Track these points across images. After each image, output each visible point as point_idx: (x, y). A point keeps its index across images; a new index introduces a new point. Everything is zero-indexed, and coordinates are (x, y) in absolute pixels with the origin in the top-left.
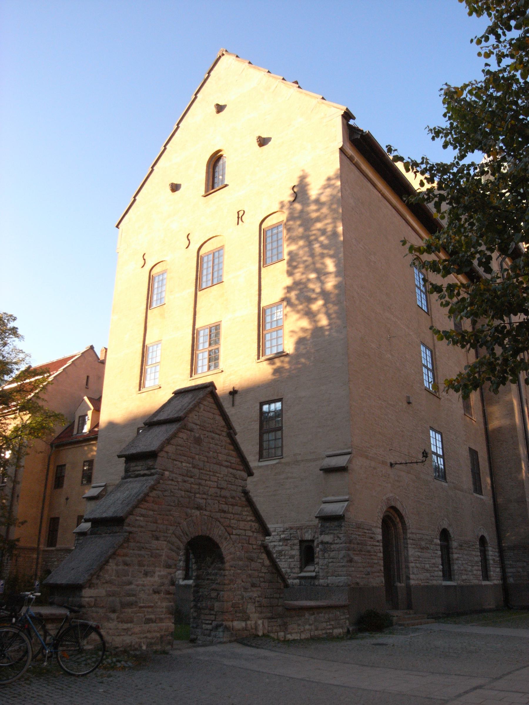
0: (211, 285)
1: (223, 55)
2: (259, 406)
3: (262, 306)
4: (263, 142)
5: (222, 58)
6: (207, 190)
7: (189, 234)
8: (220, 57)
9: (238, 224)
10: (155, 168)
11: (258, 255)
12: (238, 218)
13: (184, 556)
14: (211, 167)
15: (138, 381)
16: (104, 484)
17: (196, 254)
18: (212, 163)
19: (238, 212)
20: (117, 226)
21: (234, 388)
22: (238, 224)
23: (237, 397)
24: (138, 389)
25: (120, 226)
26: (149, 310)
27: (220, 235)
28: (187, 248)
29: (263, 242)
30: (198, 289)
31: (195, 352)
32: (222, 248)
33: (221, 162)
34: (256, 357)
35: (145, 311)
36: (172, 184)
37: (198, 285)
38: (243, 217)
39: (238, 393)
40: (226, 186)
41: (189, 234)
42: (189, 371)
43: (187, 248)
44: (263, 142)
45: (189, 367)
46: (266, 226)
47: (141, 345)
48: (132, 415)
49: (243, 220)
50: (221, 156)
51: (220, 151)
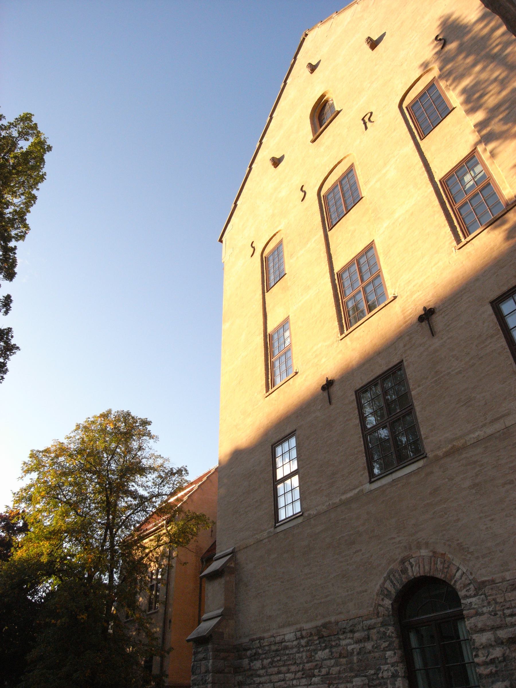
0: (345, 212)
1: (306, 35)
2: (490, 308)
3: (437, 180)
4: (373, 44)
5: (306, 39)
6: (314, 130)
7: (303, 186)
8: (304, 39)
9: (366, 128)
10: (253, 166)
11: (408, 134)
12: (365, 123)
13: (401, 665)
14: (316, 121)
15: (264, 382)
16: (230, 550)
17: (316, 197)
18: (317, 114)
19: (363, 119)
20: (221, 241)
21: (425, 308)
22: (366, 128)
23: (437, 320)
24: (265, 391)
25: (224, 239)
26: (266, 294)
27: (345, 158)
28: (302, 200)
29: (411, 118)
30: (327, 228)
31: (341, 301)
32: (351, 170)
33: (327, 107)
34: (455, 243)
35: (261, 297)
36: (273, 157)
37: (327, 226)
38: (372, 119)
39: (436, 311)
40: (339, 112)
41: (303, 186)
42: (337, 329)
43: (302, 200)
44: (373, 44)
45: (336, 323)
46: (410, 102)
47: (262, 335)
48: (262, 430)
49: (372, 121)
50: (327, 101)
51: (323, 96)
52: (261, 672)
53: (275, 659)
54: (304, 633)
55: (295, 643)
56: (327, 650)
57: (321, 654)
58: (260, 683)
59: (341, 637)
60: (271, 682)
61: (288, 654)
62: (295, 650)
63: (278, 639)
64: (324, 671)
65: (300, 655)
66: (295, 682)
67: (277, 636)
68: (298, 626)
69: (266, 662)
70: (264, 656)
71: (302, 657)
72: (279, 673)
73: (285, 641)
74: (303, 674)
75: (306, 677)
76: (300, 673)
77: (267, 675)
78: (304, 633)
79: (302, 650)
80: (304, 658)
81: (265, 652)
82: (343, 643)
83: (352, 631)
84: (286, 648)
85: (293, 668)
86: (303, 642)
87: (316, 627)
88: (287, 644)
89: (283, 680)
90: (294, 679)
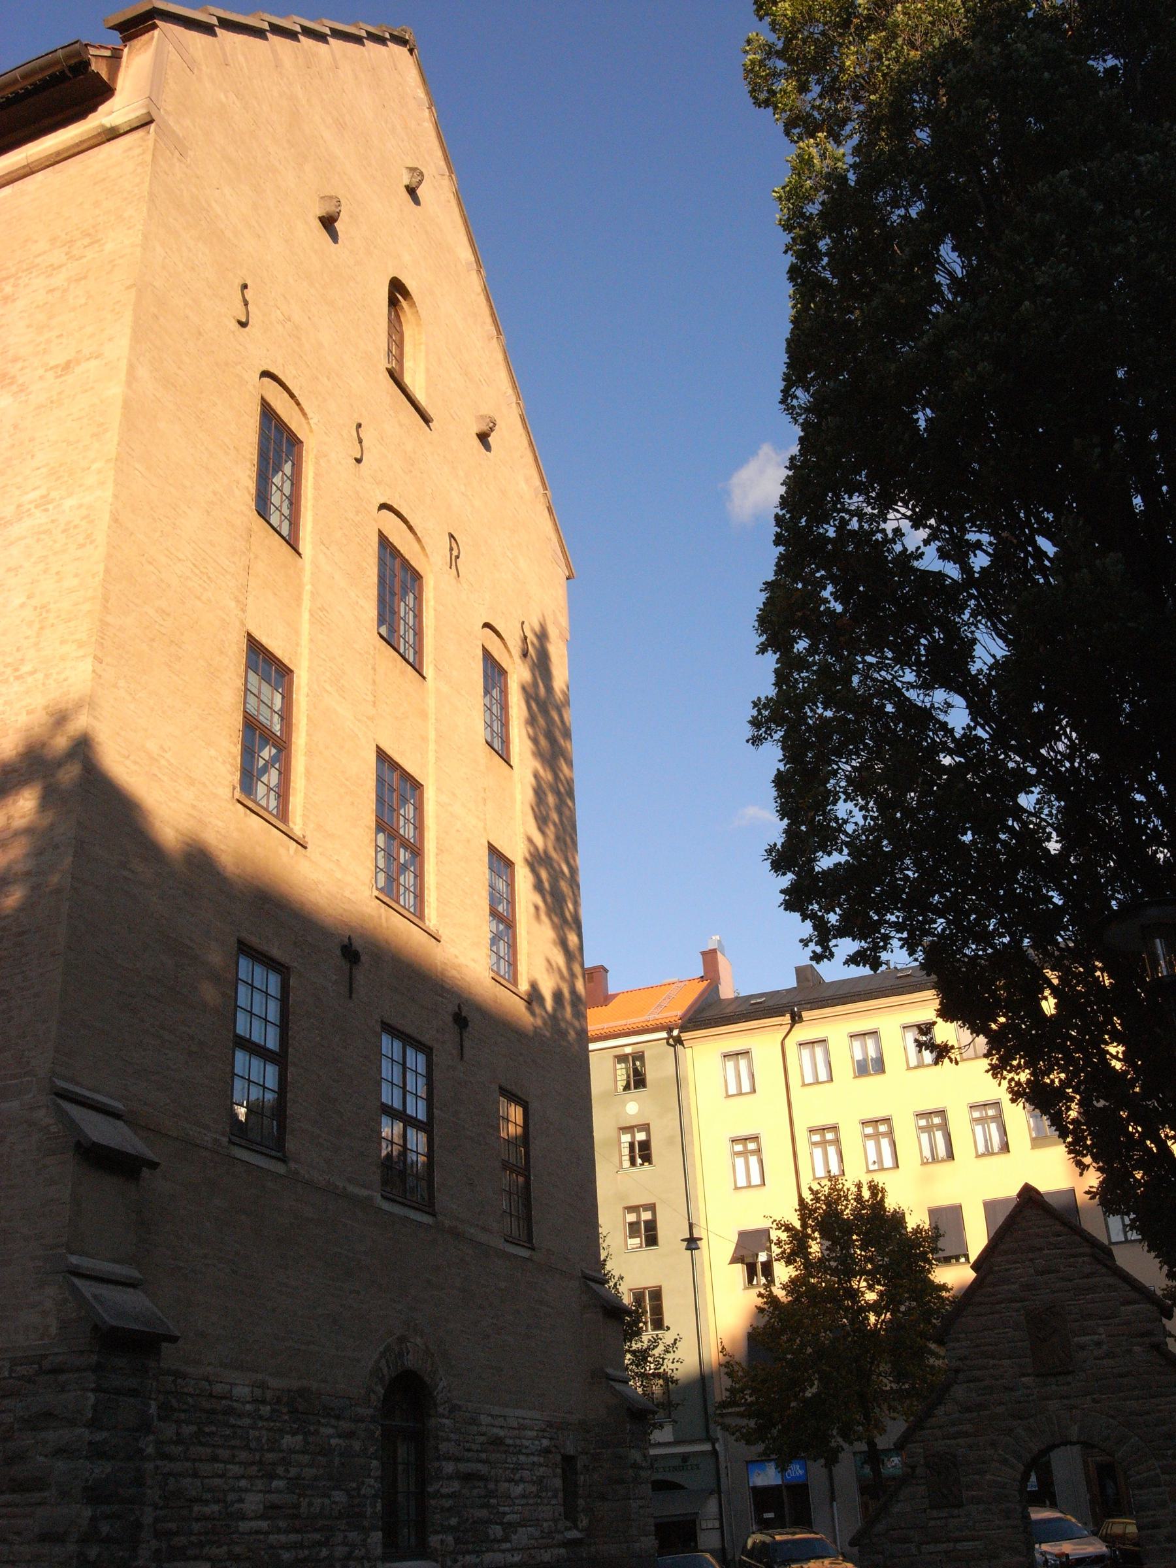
52: (177, 1450)
53: (207, 1430)
54: (269, 1395)
55: (248, 1407)
56: (300, 1437)
57: (288, 1441)
58: (170, 1474)
59: (323, 1421)
60: (195, 1475)
61: (233, 1426)
62: (247, 1421)
63: (219, 1389)
64: (293, 1471)
65: (257, 1433)
66: (243, 1483)
67: (217, 1382)
68: (260, 1377)
69: (188, 1430)
70: (183, 1416)
71: (258, 1439)
72: (215, 1459)
73: (231, 1399)
74: (259, 1471)
75: (262, 1477)
76: (255, 1468)
77: (187, 1460)
78: (269, 1395)
79: (260, 1424)
80: (264, 1441)
81: (185, 1407)
82: (323, 1430)
83: (338, 1418)
84: (230, 1411)
85: (243, 1455)
86: (266, 1410)
87: (289, 1391)
88: (235, 1404)
89: (221, 1476)
90: (243, 1477)
